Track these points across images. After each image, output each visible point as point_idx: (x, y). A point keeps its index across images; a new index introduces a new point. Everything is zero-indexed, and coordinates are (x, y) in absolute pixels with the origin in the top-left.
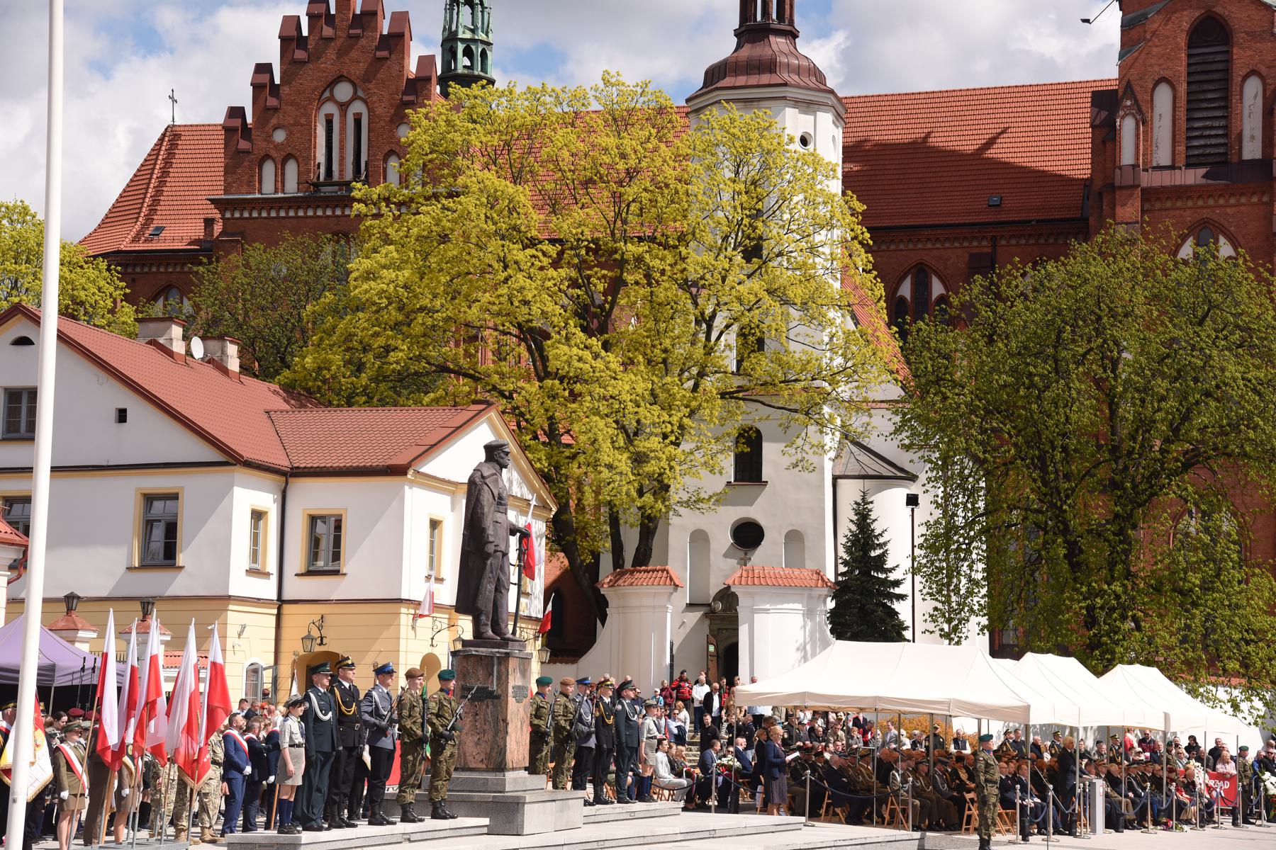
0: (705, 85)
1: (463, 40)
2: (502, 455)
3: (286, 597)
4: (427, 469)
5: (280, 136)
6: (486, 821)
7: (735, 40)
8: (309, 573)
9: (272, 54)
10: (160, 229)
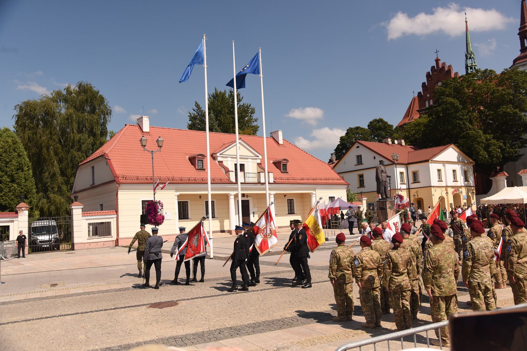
0: (513, 63)
1: (469, 66)
3: (410, 188)
4: (434, 160)
5: (428, 95)
7: (520, 52)
8: (414, 183)
9: (425, 80)
10: (413, 117)
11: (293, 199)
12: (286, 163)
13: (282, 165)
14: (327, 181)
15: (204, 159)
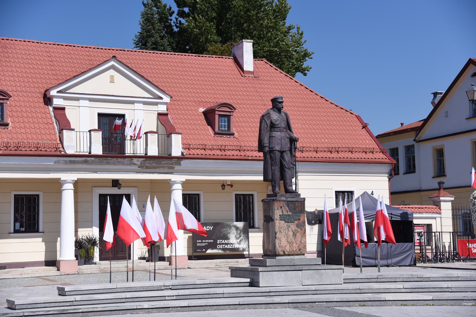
2: (277, 103)
6: (248, 280)
11: (252, 195)
12: (229, 114)
13: (217, 117)
14: (335, 155)
15: (5, 101)
